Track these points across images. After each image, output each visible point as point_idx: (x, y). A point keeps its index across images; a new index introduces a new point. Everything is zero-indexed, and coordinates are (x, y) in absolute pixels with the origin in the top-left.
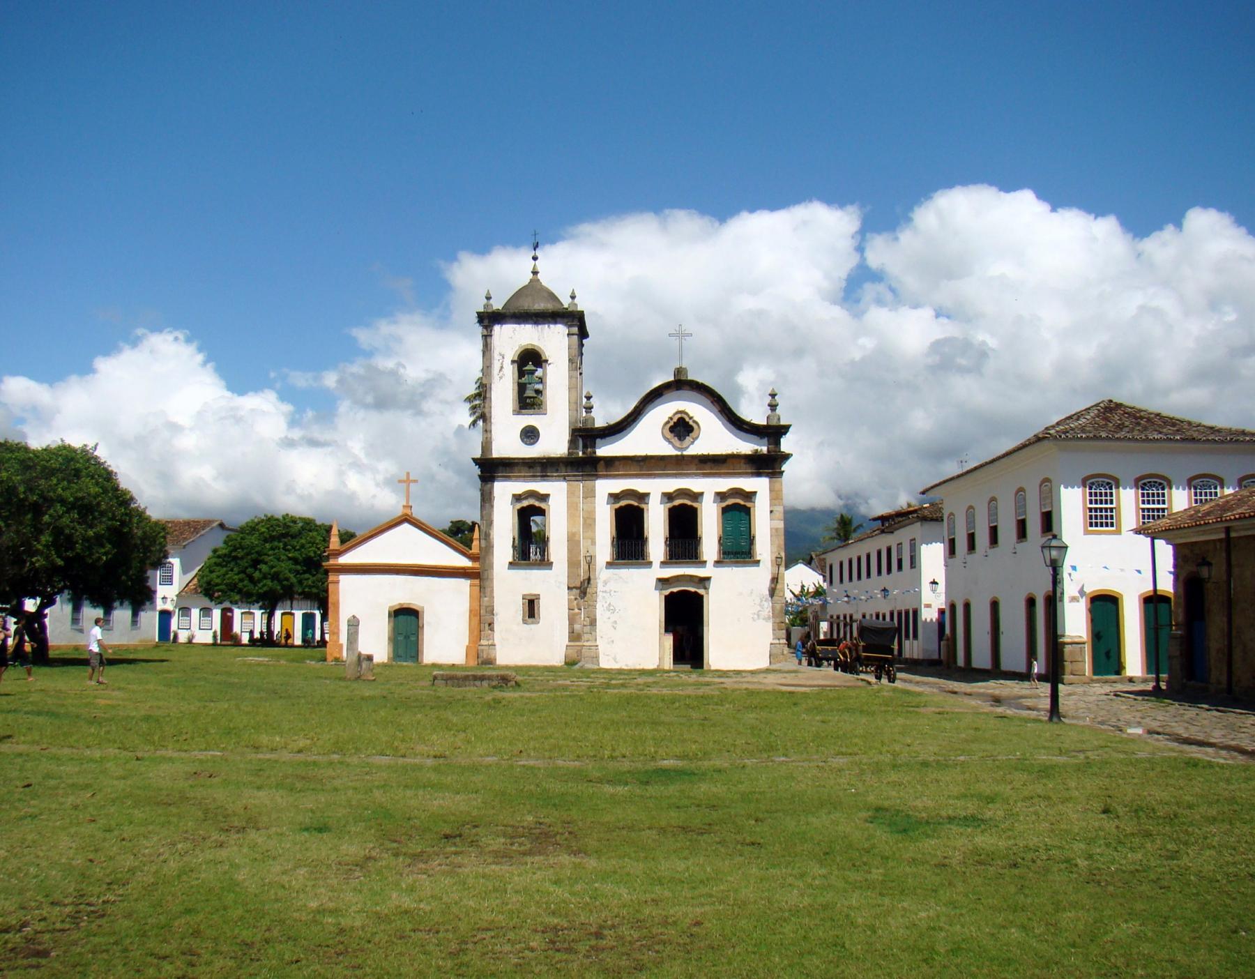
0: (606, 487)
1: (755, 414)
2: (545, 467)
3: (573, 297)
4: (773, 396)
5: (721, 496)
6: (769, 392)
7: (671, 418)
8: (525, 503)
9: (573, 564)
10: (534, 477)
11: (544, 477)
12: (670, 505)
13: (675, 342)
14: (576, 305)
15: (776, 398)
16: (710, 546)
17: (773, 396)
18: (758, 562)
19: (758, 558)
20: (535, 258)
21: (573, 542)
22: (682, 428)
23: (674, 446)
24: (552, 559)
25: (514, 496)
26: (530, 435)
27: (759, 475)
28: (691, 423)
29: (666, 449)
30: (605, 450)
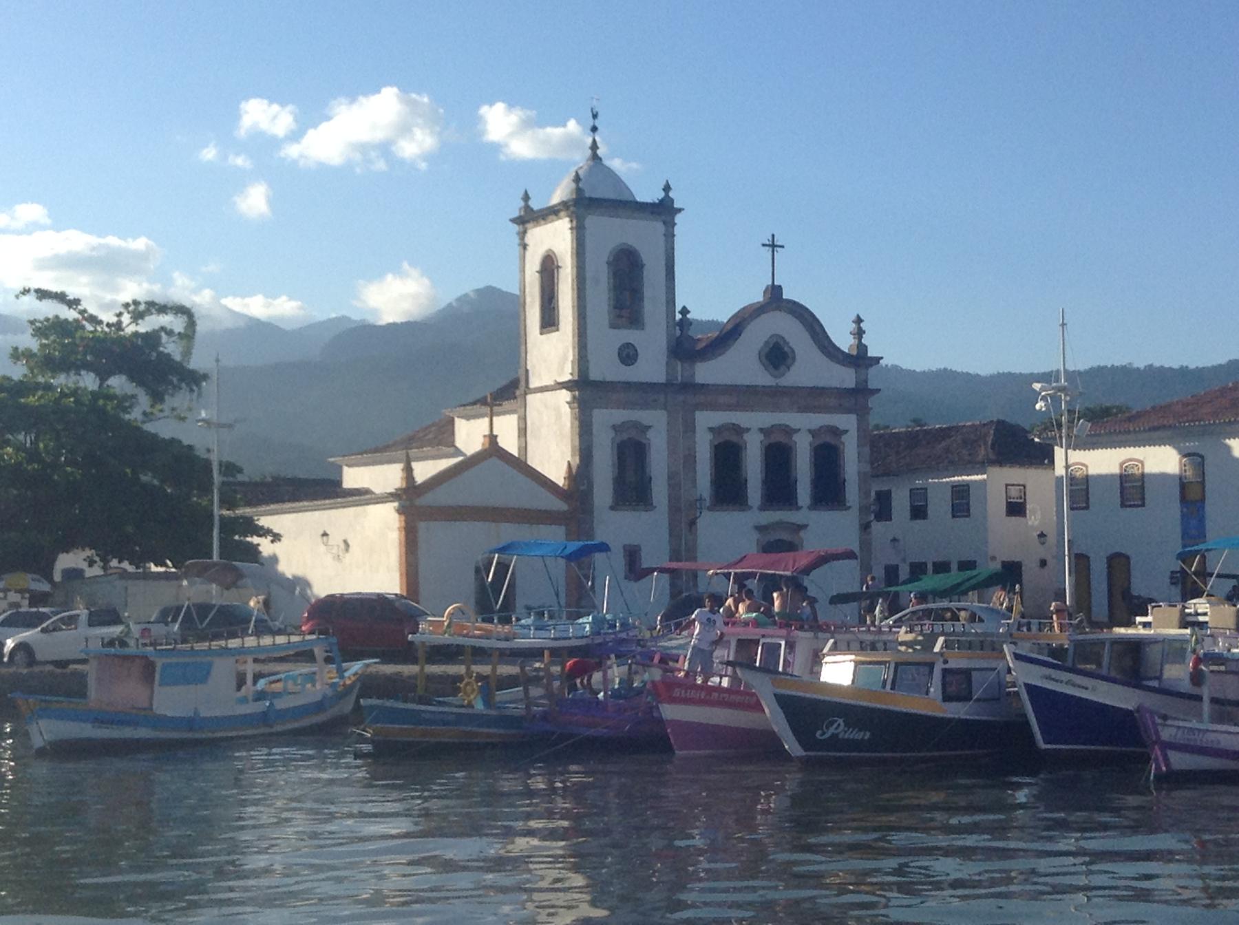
0: (707, 420)
1: (844, 341)
2: (644, 393)
3: (667, 188)
4: (859, 320)
5: (814, 433)
6: (854, 317)
7: (767, 343)
8: (625, 436)
9: (674, 509)
10: (631, 405)
11: (645, 406)
12: (767, 443)
13: (767, 252)
14: (672, 201)
15: (862, 325)
16: (804, 492)
17: (859, 320)
18: (850, 507)
19: (848, 505)
20: (594, 129)
21: (674, 484)
22: (777, 356)
23: (772, 375)
24: (654, 504)
25: (614, 427)
26: (628, 355)
27: (849, 411)
28: (786, 349)
29: (761, 377)
30: (706, 372)
